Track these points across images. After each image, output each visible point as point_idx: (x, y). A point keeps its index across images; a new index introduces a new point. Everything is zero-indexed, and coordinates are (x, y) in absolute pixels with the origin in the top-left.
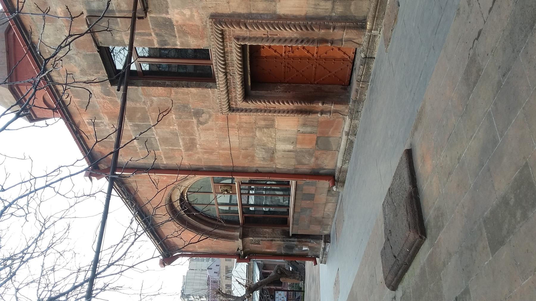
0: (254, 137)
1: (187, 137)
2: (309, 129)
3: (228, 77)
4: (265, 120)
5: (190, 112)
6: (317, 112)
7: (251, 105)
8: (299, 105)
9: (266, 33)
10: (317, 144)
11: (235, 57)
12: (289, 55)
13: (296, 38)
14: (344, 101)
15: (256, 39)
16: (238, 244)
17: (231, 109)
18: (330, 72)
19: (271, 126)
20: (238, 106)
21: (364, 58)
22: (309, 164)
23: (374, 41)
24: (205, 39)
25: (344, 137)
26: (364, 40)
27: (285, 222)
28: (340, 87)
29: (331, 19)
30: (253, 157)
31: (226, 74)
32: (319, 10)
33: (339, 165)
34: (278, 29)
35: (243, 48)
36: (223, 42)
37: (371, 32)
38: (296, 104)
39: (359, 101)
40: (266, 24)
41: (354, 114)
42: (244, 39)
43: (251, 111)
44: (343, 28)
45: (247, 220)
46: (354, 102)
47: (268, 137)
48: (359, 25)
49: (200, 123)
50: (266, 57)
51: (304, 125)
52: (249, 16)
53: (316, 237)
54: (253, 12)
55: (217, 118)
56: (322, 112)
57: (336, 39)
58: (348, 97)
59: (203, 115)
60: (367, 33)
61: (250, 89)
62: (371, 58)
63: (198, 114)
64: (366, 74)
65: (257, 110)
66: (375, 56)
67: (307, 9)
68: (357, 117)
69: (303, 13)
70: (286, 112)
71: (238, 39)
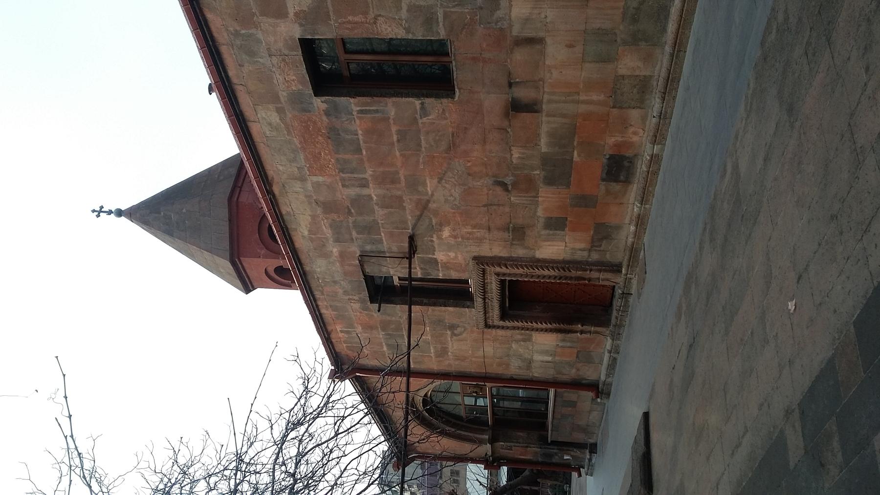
0: (510, 348)
1: (439, 346)
2: (569, 344)
4: (522, 334)
6: (577, 332)
7: (508, 324)
10: (577, 357)
14: (605, 323)
15: (515, 275)
16: (487, 448)
17: (487, 326)
19: (528, 339)
22: (570, 374)
25: (607, 355)
27: (543, 426)
30: (508, 365)
33: (603, 378)
35: (502, 282)
39: (619, 326)
40: (526, 266)
41: (616, 336)
42: (504, 275)
43: (508, 328)
44: (600, 271)
45: (496, 421)
46: (615, 326)
48: (616, 268)
49: (453, 334)
51: (563, 340)
53: (581, 446)
55: (472, 332)
56: (582, 332)
58: (610, 320)
63: (452, 327)
64: (625, 305)
65: (514, 328)
69: (561, 258)
71: (498, 274)
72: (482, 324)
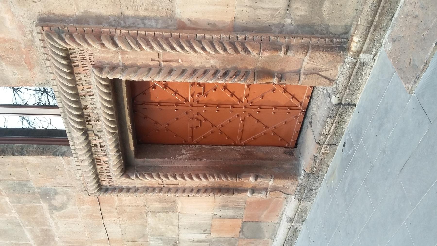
0: (145, 225)
1: (37, 229)
2: (231, 213)
3: (91, 138)
4: (160, 201)
5: (34, 193)
7: (135, 181)
8: (217, 180)
9: (156, 58)
10: (242, 231)
11: (98, 103)
12: (200, 99)
13: (213, 67)
14: (291, 173)
15: (136, 68)
18: (266, 127)
19: (171, 209)
20: (114, 184)
21: (335, 105)
23: (359, 74)
24: (37, 69)
26: (341, 72)
28: (282, 149)
29: (282, 30)
31: (85, 132)
32: (260, 12)
34: (178, 49)
35: (114, 86)
36: (71, 73)
37: (358, 56)
38: (211, 180)
39: (314, 175)
40: (155, 38)
41: (306, 193)
42: (113, 68)
43: (137, 190)
44: (305, 48)
46: (308, 175)
47: (167, 224)
49: (53, 208)
50: (159, 103)
51: (224, 207)
52: (120, 21)
54: (128, 13)
56: (254, 190)
57: (287, 69)
59: (57, 197)
60: (349, 58)
61: (133, 155)
62: (349, 104)
63: (47, 195)
65: (147, 189)
66: (357, 102)
67: (237, 9)
68: (309, 198)
70: (195, 190)
72: (92, 185)
